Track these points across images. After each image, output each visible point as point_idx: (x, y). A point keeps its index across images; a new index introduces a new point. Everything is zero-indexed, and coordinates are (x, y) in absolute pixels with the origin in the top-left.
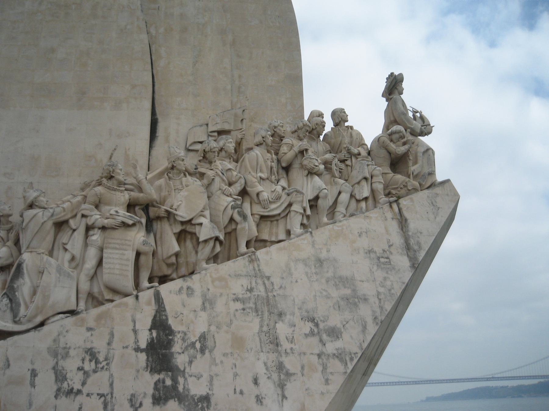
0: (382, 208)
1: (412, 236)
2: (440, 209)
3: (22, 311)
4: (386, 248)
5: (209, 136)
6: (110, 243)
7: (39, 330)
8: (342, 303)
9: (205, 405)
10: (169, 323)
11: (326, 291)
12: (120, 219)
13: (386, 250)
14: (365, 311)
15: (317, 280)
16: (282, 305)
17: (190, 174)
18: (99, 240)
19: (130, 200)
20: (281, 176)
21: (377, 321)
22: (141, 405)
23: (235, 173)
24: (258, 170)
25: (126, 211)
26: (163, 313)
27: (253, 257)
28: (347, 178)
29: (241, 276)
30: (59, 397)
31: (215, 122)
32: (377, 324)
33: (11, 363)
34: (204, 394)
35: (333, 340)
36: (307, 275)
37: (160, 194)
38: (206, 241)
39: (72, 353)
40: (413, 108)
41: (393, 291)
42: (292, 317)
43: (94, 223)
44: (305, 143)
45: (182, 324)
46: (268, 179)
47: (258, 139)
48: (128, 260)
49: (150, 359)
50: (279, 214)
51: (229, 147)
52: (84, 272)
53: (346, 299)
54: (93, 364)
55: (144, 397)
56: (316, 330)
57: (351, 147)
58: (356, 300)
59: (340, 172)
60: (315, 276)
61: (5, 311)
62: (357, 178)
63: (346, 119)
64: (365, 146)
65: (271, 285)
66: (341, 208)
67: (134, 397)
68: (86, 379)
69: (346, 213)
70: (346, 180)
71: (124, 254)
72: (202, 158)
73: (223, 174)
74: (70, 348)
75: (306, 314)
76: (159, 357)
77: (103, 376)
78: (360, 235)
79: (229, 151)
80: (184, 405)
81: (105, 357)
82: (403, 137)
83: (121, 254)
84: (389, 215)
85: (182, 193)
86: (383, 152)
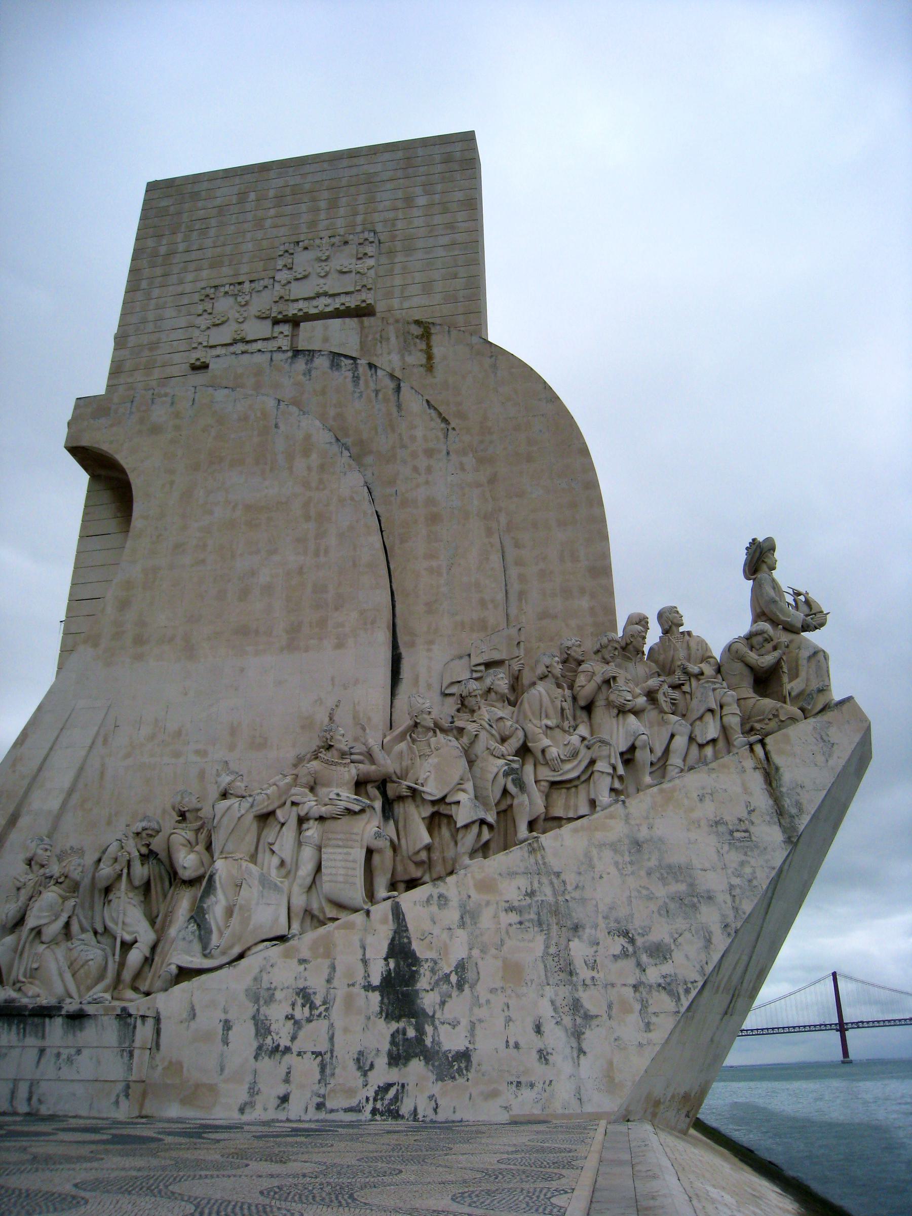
0: (737, 753)
1: (788, 794)
2: (835, 747)
3: (215, 939)
4: (744, 814)
5: (472, 671)
6: (329, 839)
7: (235, 966)
8: (672, 906)
9: (463, 1065)
10: (412, 948)
11: (648, 889)
12: (343, 804)
13: (744, 819)
14: (710, 916)
15: (633, 873)
16: (579, 914)
17: (443, 730)
18: (316, 835)
19: (358, 775)
20: (579, 720)
21: (729, 930)
22: (372, 1066)
23: (509, 723)
24: (543, 715)
25: (354, 792)
26: (405, 935)
27: (535, 845)
28: (684, 713)
29: (516, 874)
30: (260, 1058)
31: (479, 652)
32: (729, 935)
33: (198, 1011)
34: (462, 1048)
35: (658, 963)
36: (617, 867)
37: (401, 764)
38: (467, 826)
39: (279, 995)
40: (793, 589)
41: (755, 883)
42: (593, 931)
43: (307, 814)
44: (611, 670)
45: (431, 949)
46: (558, 727)
47: (541, 670)
48: (354, 861)
49: (386, 1001)
50: (578, 777)
51: (499, 685)
52: (298, 881)
53: (679, 899)
54: (307, 1009)
55: (377, 1055)
56: (631, 949)
57: (688, 664)
58: (695, 900)
59: (673, 704)
60: (629, 866)
61: (191, 942)
62: (698, 710)
63: (680, 622)
64: (711, 660)
65: (562, 884)
66: (675, 760)
67: (363, 1055)
68: (297, 1032)
69: (684, 765)
70: (684, 716)
71: (349, 854)
72: (460, 706)
73: (491, 726)
74: (275, 989)
75: (616, 924)
76: (398, 997)
77: (321, 1026)
78: (701, 799)
79: (500, 691)
80: (433, 1065)
81: (322, 1000)
82: (769, 640)
83: (345, 854)
84: (749, 763)
85: (430, 760)
86: (739, 666)
